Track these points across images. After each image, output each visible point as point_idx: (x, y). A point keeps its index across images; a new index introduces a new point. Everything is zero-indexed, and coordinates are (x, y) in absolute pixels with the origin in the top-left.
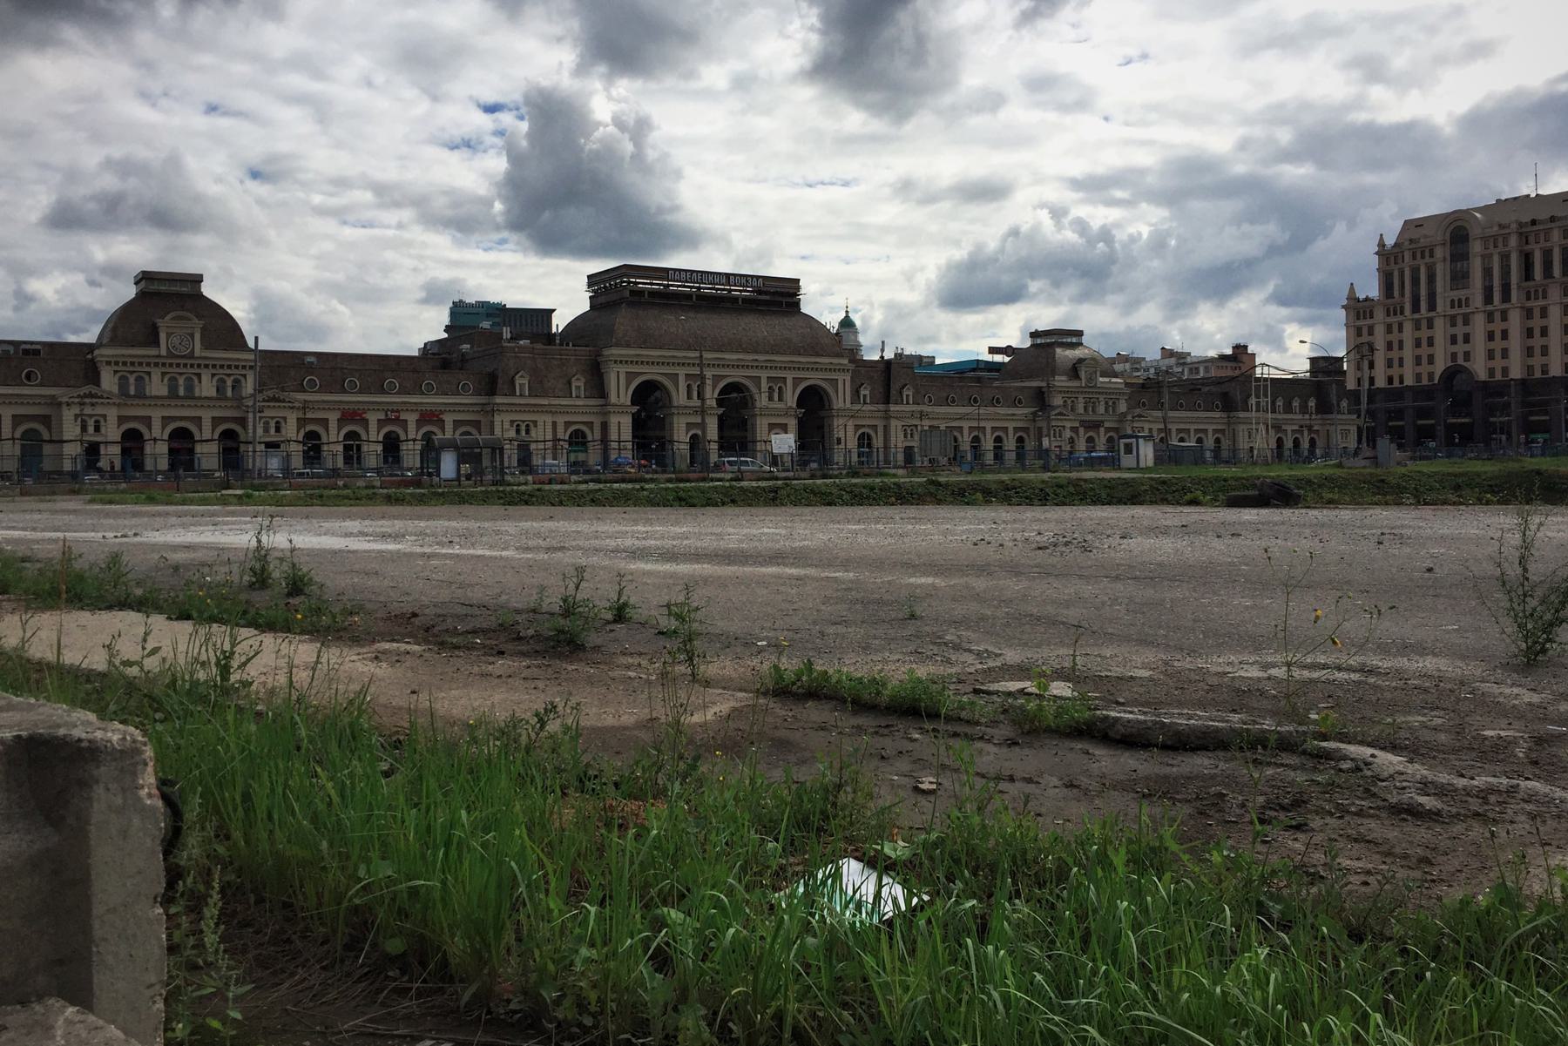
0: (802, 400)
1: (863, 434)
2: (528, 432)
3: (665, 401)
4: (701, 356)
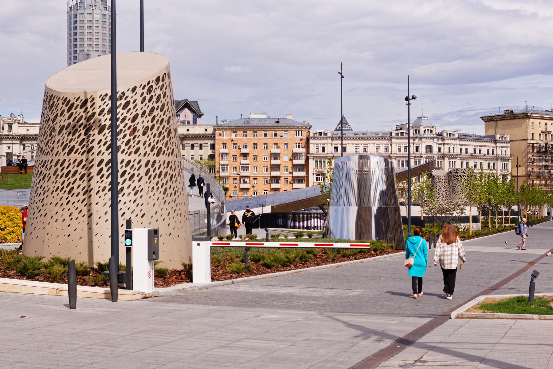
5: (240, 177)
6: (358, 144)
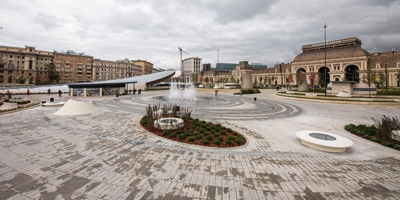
0: (347, 69)
1: (287, 79)
2: (277, 79)
3: (328, 70)
4: (325, 61)
5: (65, 72)
6: (110, 64)
